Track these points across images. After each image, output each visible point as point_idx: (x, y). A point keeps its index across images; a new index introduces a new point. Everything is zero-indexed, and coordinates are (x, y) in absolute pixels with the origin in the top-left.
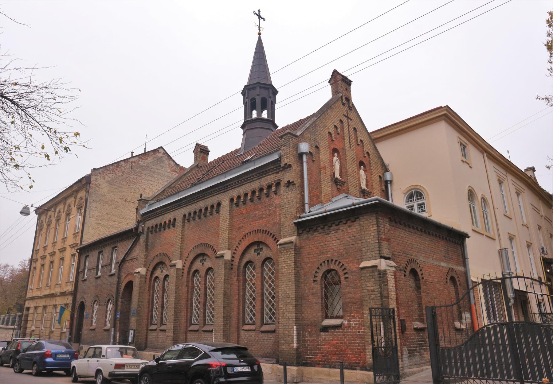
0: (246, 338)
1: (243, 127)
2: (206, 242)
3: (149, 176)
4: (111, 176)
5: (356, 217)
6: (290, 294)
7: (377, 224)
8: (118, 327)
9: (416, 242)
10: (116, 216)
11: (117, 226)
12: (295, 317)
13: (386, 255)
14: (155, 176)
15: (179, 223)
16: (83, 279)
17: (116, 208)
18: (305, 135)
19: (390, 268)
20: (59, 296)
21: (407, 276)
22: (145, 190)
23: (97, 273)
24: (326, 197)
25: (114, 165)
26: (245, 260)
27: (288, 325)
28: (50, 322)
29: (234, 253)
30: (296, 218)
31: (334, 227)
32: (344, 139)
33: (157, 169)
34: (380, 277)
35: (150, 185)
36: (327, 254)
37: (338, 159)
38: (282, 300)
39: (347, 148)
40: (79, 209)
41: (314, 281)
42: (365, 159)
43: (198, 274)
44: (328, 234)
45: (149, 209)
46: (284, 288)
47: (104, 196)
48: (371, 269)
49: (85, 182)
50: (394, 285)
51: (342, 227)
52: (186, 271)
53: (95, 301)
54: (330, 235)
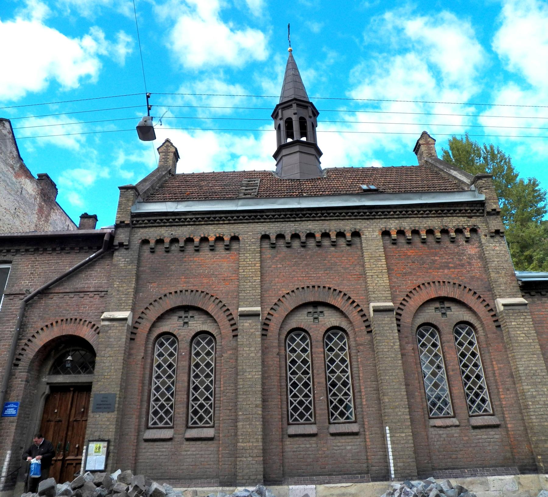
0: (442, 439)
38: (526, 378)
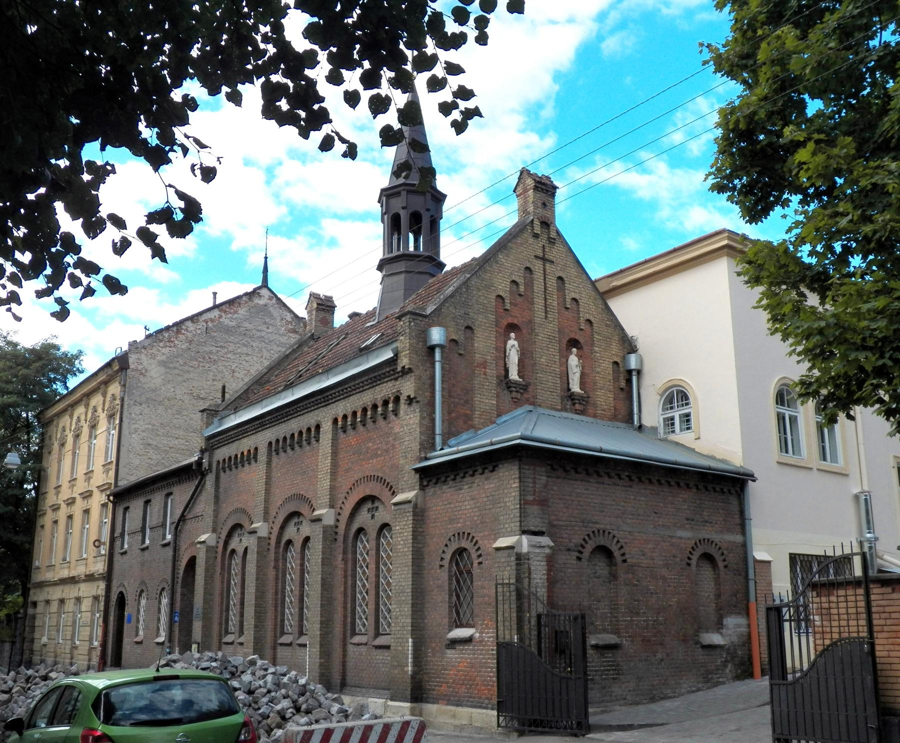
0: (355, 657)
1: (380, 268)
2: (301, 493)
4: (166, 350)
5: (494, 464)
6: (406, 587)
7: (520, 478)
8: (177, 638)
9: (613, 500)
10: (180, 428)
11: (183, 447)
12: (410, 625)
13: (533, 529)
14: (254, 345)
15: (262, 456)
16: (122, 551)
17: (179, 412)
18: (443, 310)
19: (538, 551)
20: (84, 581)
21: (583, 560)
23: (143, 541)
24: (484, 417)
25: (171, 329)
26: (355, 527)
27: (402, 636)
29: (339, 514)
31: (468, 479)
32: (532, 303)
33: (258, 330)
34: (517, 564)
35: (244, 363)
36: (458, 523)
37: (516, 343)
39: (537, 320)
40: (111, 417)
41: (441, 566)
42: (581, 333)
43: (293, 546)
44: (461, 489)
45: (220, 426)
46: (399, 577)
47: (154, 390)
48: (507, 551)
49: (117, 368)
50: (546, 577)
51: (478, 479)
53: (142, 591)
54: (463, 491)
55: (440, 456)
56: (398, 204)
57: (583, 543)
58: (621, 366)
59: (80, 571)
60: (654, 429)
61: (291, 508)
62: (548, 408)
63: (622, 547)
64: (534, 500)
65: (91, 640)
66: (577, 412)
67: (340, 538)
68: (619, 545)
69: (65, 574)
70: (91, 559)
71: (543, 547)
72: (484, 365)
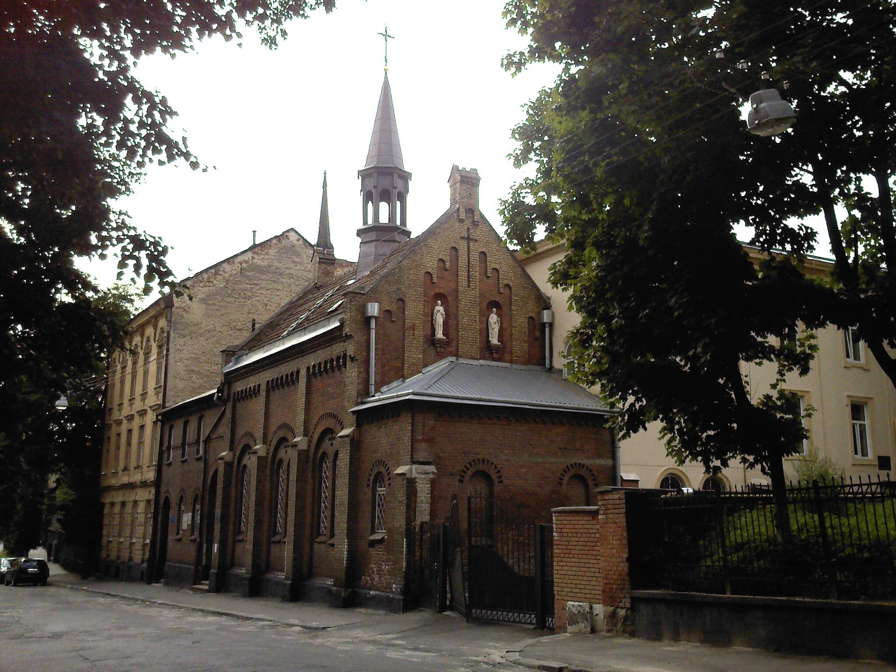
3: (272, 283)
13: (421, 460)
18: (379, 288)
20: (140, 487)
22: (268, 307)
26: (321, 451)
28: (118, 527)
30: (358, 404)
40: (160, 347)
45: (236, 363)
50: (430, 495)
52: (269, 460)
55: (378, 399)
56: (371, 183)
57: (465, 469)
58: (536, 320)
59: (136, 478)
60: (561, 371)
61: (281, 434)
62: (468, 358)
63: (499, 471)
64: (423, 438)
65: (144, 537)
66: (494, 360)
67: (311, 460)
68: (496, 470)
69: (125, 480)
70: (145, 469)
71: (429, 473)
72: (413, 327)
